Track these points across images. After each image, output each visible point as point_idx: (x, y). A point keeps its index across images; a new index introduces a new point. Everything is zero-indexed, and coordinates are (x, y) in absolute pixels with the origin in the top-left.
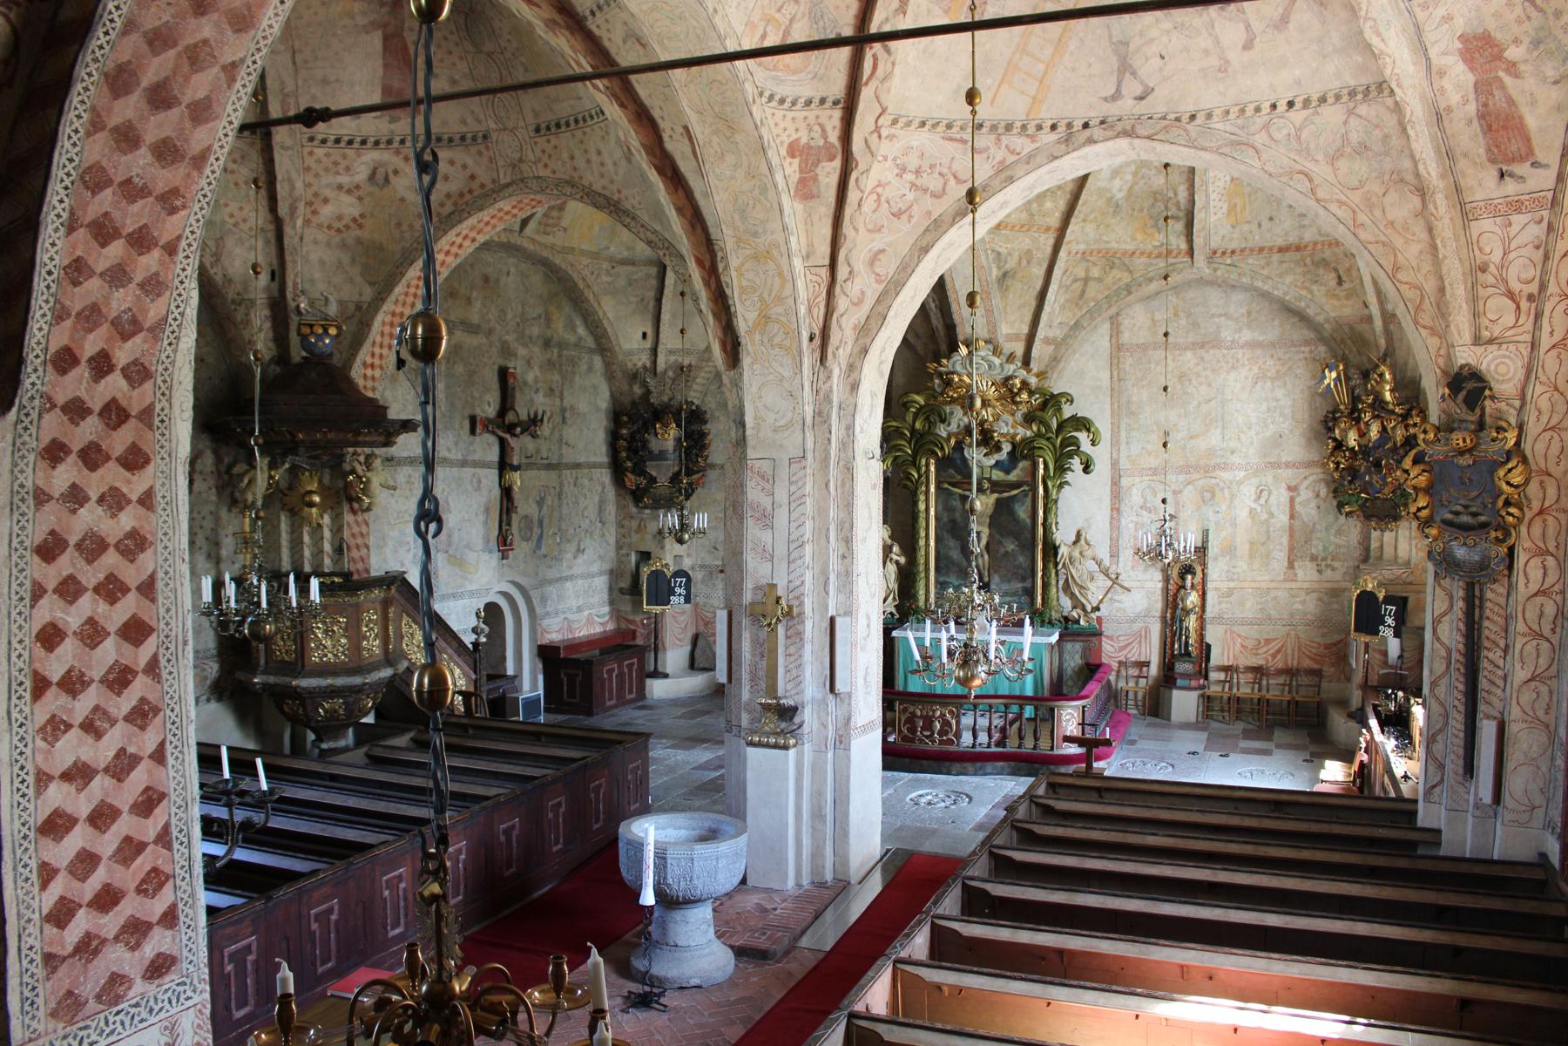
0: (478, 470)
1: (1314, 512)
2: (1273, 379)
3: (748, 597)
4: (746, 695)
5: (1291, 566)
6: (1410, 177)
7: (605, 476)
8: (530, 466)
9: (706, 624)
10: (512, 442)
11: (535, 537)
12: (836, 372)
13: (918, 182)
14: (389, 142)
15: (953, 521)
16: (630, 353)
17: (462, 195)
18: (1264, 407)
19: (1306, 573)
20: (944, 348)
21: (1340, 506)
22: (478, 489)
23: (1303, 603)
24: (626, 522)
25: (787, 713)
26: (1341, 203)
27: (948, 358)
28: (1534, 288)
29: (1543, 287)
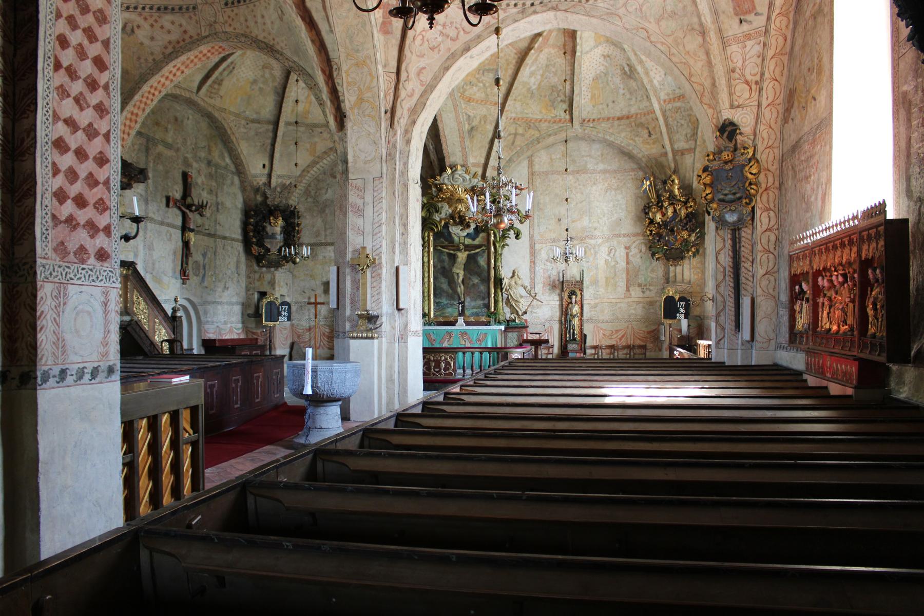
0: (170, 229)
1: (639, 260)
2: (615, 190)
3: (349, 256)
4: (348, 312)
5: (628, 289)
6: (697, 27)
7: (240, 247)
8: (198, 233)
9: (298, 337)
10: (190, 215)
11: (201, 275)
12: (399, 133)
13: (444, 31)
14: (136, 8)
15: (443, 268)
16: (256, 176)
17: (178, 42)
18: (611, 204)
19: (636, 293)
20: (437, 171)
21: (653, 255)
22: (170, 240)
23: (635, 309)
24: (252, 275)
25: (372, 319)
26: (663, 43)
27: (441, 176)
28: (758, 78)
29: (762, 75)
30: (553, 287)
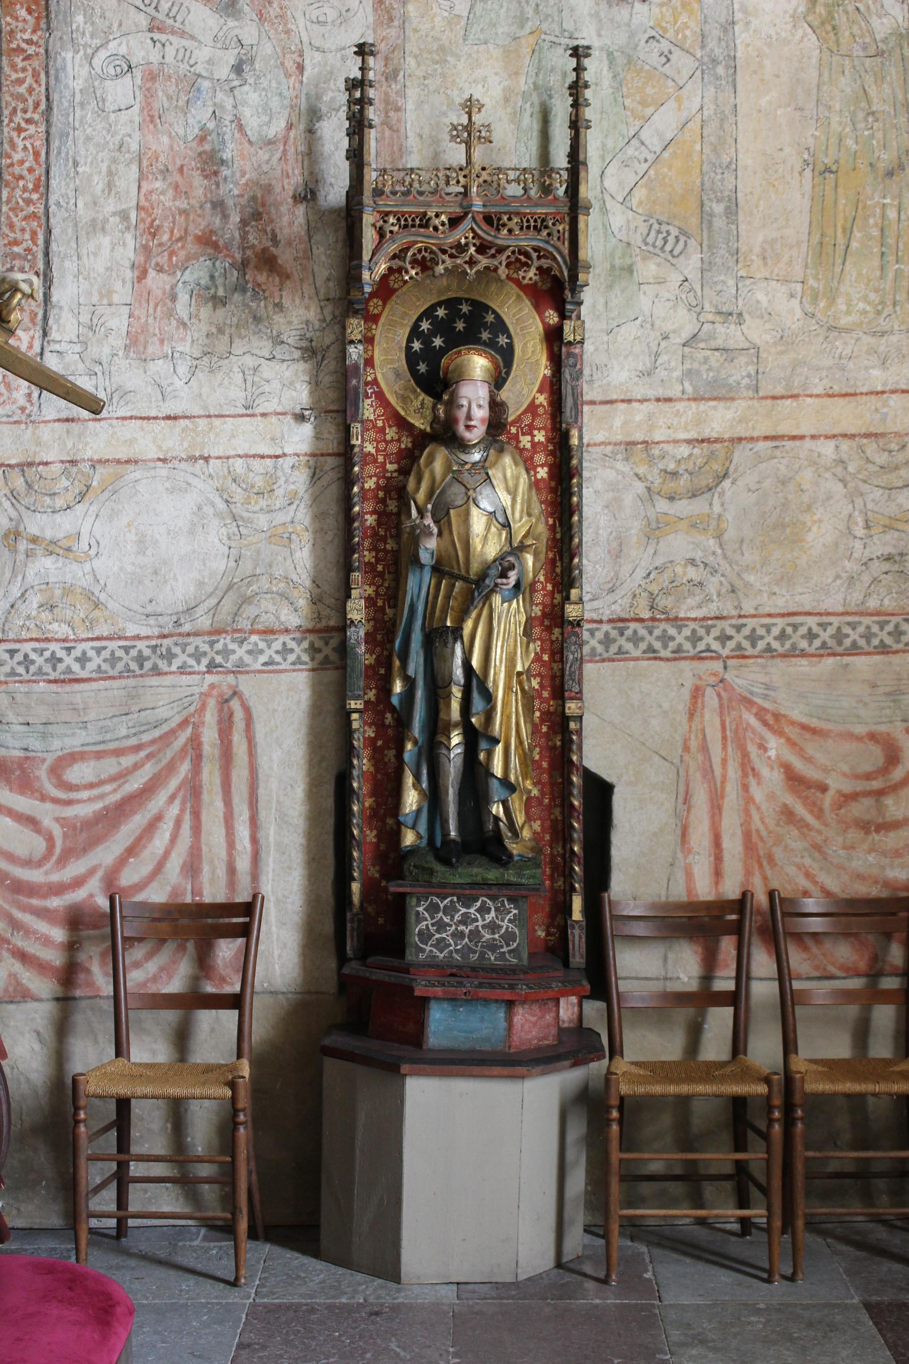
30: (248, 265)
